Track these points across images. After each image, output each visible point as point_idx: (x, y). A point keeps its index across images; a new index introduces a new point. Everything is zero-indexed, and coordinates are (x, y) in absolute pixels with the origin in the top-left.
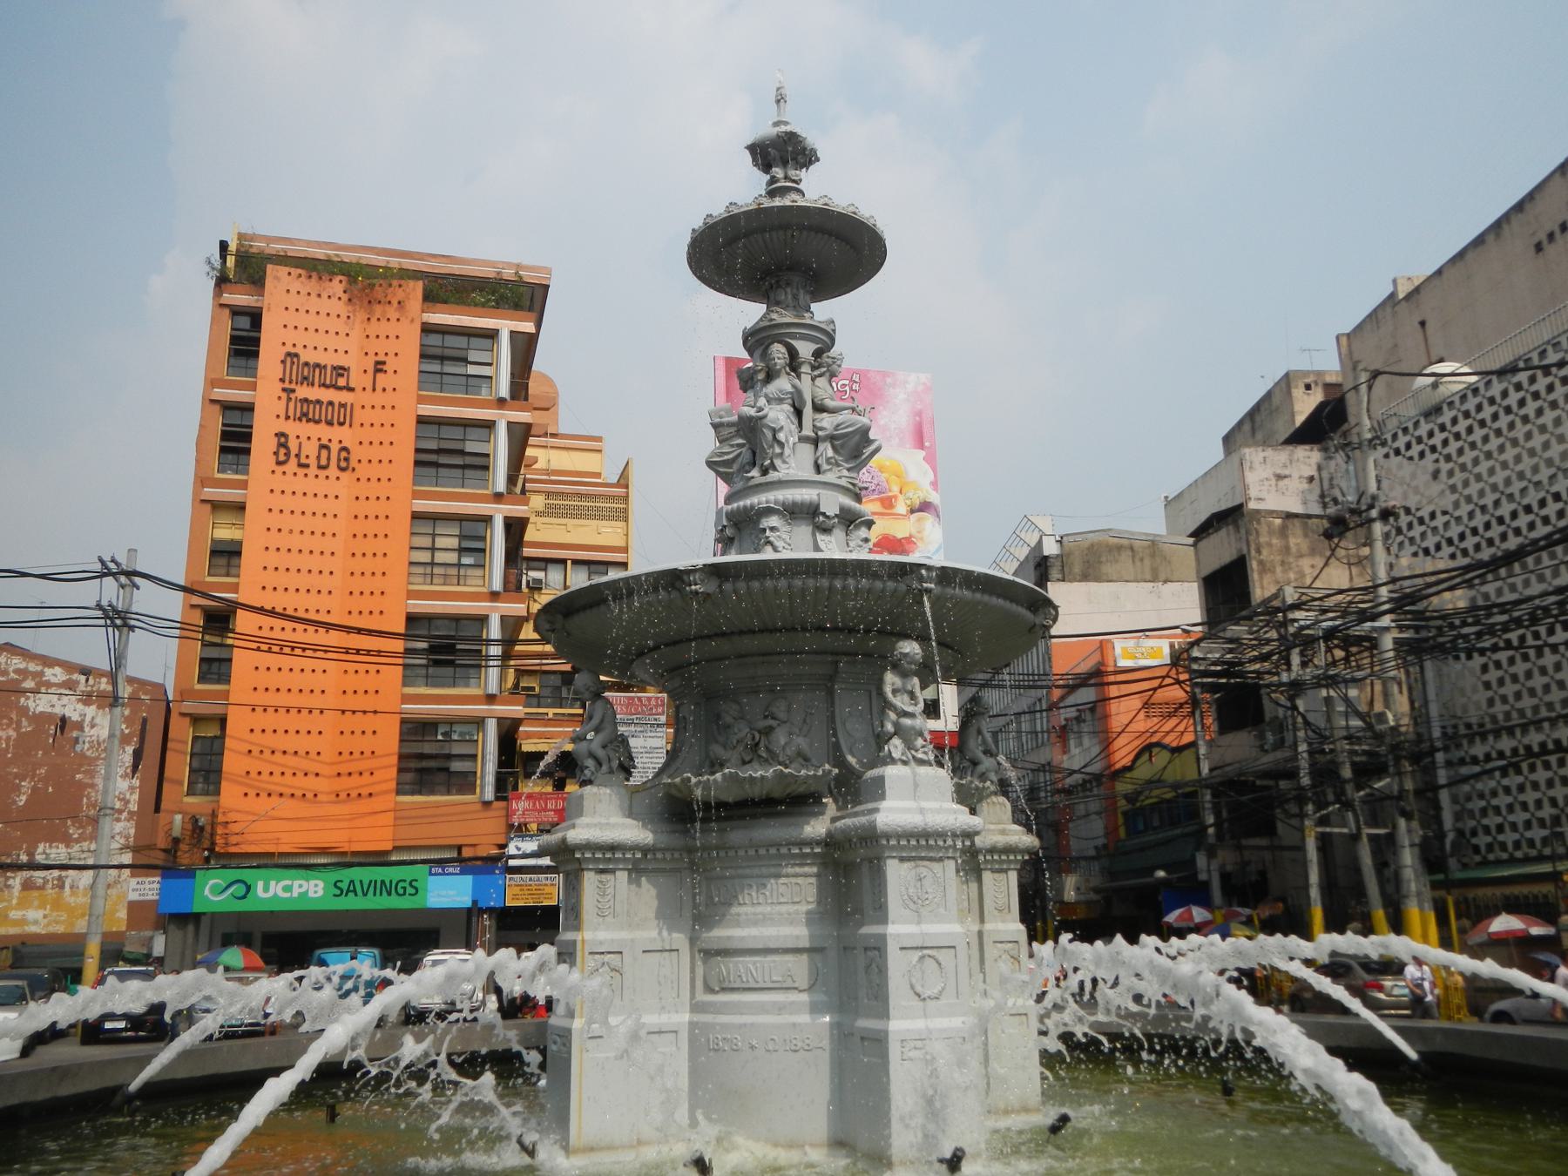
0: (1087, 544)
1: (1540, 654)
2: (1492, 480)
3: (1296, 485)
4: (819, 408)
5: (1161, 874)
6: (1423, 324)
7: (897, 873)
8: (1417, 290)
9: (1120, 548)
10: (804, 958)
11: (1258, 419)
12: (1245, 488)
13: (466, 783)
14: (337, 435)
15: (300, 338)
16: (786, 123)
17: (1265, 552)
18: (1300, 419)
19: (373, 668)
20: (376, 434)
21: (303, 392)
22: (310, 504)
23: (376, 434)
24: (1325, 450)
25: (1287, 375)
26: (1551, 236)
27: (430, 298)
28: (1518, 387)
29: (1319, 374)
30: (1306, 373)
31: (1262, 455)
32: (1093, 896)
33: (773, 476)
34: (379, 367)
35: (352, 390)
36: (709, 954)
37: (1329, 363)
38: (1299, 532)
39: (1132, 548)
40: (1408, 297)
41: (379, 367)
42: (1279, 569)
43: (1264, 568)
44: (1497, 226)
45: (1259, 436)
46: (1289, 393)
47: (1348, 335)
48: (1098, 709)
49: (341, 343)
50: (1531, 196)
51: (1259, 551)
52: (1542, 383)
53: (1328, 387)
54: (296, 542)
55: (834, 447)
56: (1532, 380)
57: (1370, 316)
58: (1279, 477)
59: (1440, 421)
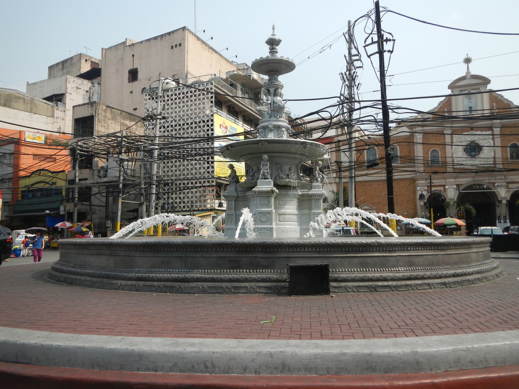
0: (7, 93)
1: (184, 161)
2: (179, 114)
3: (82, 92)
5: (48, 212)
6: (133, 56)
8: (133, 45)
9: (20, 98)
10: (296, 216)
11: (65, 65)
12: (66, 89)
16: (275, 35)
17: (100, 116)
24: (93, 83)
25: (80, 54)
26: (176, 45)
28: (191, 92)
29: (90, 57)
30: (87, 56)
31: (73, 79)
32: (4, 219)
33: (281, 119)
36: (280, 215)
37: (97, 56)
38: (109, 112)
39: (24, 99)
40: (130, 46)
42: (103, 122)
43: (99, 121)
44: (162, 36)
45: (65, 71)
46: (80, 61)
47: (106, 49)
48: (16, 155)
50: (173, 32)
51: (98, 115)
52: (197, 93)
53: (92, 62)
56: (195, 91)
57: (115, 46)
58: (77, 88)
59: (167, 94)
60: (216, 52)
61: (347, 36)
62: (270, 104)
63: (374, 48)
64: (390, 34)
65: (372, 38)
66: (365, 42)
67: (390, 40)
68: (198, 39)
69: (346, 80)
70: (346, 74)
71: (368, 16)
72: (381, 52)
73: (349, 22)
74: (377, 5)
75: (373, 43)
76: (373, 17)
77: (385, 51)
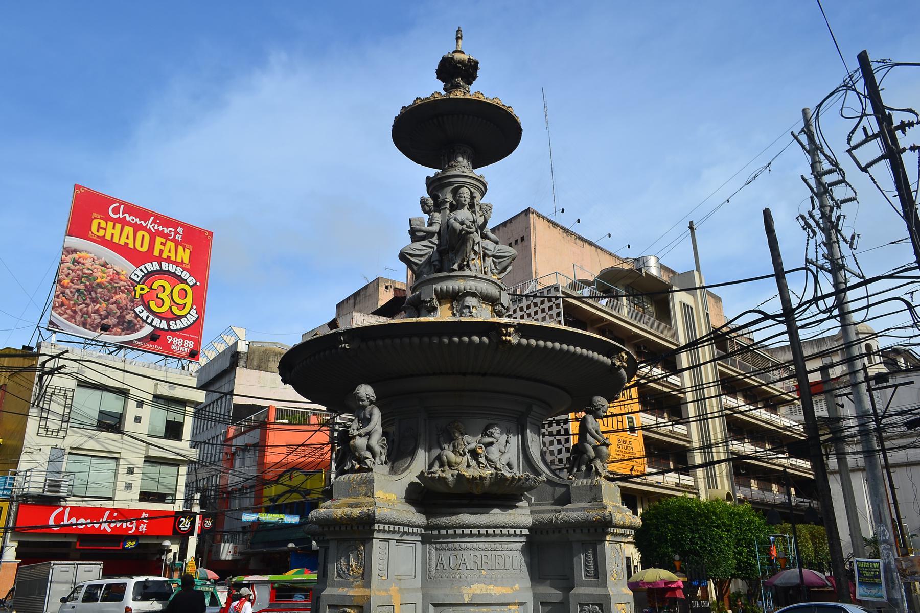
11: (358, 299)
18: (381, 303)
26: (516, 241)
29: (393, 282)
33: (467, 272)
45: (357, 307)
50: (510, 221)
53: (395, 288)
55: (494, 262)
60: (590, 243)
61: (804, 138)
62: (439, 233)
63: (874, 149)
64: (910, 111)
65: (864, 129)
66: (849, 141)
67: (911, 124)
68: (555, 225)
69: (817, 230)
70: (811, 216)
71: (848, 86)
72: (893, 155)
73: (804, 112)
74: (863, 58)
75: (868, 139)
76: (860, 86)
77: (904, 150)
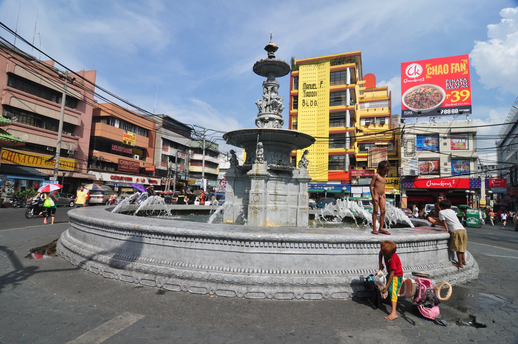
4: (271, 99)
7: (253, 182)
13: (344, 167)
14: (314, 98)
15: (306, 80)
19: (322, 145)
20: (322, 97)
21: (307, 91)
22: (309, 113)
23: (322, 97)
27: (332, 64)
34: (321, 83)
35: (316, 88)
41: (321, 83)
49: (314, 79)
54: (307, 121)
